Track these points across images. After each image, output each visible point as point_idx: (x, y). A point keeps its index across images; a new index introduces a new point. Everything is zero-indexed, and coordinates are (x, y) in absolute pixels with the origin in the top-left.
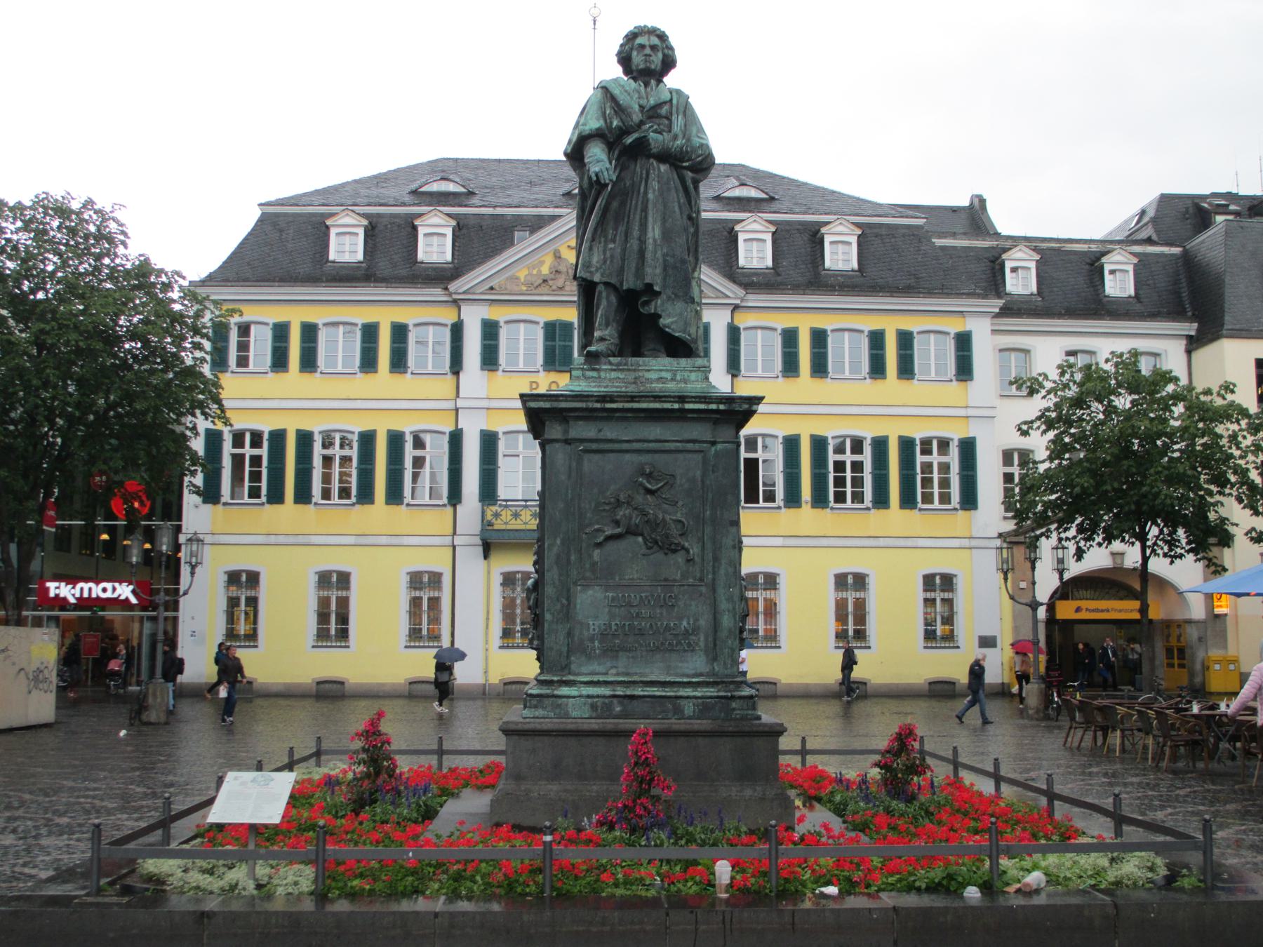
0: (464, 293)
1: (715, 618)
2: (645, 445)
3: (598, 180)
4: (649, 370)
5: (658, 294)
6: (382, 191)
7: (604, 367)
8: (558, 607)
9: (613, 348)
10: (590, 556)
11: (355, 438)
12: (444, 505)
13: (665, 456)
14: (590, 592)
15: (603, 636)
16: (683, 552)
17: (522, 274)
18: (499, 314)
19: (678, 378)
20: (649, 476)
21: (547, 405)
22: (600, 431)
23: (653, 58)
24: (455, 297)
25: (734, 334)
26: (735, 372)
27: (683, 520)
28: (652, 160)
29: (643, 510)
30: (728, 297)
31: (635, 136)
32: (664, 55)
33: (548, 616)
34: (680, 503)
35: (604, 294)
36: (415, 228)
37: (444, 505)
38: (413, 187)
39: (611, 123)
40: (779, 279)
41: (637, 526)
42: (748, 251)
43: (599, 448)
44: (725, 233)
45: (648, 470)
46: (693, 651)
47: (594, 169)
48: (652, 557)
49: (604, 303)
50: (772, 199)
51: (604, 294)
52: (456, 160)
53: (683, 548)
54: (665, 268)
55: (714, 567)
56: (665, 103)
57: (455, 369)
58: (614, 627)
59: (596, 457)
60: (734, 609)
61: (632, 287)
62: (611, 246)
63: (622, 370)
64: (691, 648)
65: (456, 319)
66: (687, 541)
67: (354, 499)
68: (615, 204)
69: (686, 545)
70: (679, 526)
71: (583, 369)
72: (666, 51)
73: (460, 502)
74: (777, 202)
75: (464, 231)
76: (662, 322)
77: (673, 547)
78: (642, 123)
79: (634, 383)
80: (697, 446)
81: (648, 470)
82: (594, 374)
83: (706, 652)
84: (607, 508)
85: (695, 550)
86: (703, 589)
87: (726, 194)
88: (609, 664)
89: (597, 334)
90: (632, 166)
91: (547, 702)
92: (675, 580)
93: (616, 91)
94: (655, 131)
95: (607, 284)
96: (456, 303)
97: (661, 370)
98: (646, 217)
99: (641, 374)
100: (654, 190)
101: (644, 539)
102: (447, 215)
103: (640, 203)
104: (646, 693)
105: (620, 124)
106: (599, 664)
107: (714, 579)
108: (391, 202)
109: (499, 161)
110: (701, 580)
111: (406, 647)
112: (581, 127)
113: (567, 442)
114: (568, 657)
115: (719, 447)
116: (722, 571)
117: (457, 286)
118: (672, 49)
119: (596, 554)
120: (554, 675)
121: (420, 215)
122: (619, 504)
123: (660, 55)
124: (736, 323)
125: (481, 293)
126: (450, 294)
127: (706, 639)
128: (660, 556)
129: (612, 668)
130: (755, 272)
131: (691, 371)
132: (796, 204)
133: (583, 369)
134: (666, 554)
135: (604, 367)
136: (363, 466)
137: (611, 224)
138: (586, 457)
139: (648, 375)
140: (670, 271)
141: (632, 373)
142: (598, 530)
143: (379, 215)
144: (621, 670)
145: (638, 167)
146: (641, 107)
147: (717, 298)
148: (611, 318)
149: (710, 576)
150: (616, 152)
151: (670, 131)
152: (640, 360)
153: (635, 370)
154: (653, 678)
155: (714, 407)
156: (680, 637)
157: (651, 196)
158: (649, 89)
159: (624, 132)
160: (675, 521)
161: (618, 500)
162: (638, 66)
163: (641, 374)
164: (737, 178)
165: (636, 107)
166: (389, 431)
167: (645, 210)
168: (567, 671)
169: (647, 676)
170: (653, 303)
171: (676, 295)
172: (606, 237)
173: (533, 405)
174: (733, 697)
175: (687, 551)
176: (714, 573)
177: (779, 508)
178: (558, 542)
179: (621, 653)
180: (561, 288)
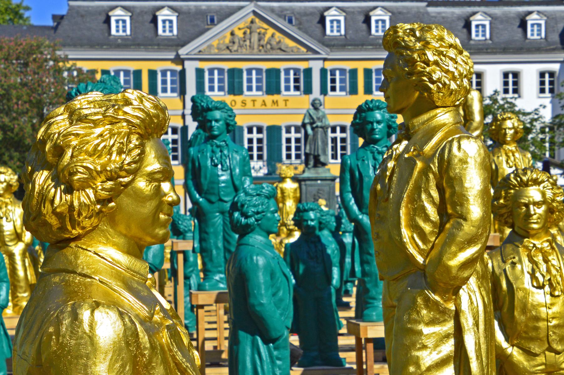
0: (187, 54)
12: (179, 164)
17: (215, 43)
18: (205, 66)
25: (323, 72)
43: (311, 185)
117: (183, 52)
125: (195, 54)
130: (334, 38)
145: (316, 129)
180: (237, 51)
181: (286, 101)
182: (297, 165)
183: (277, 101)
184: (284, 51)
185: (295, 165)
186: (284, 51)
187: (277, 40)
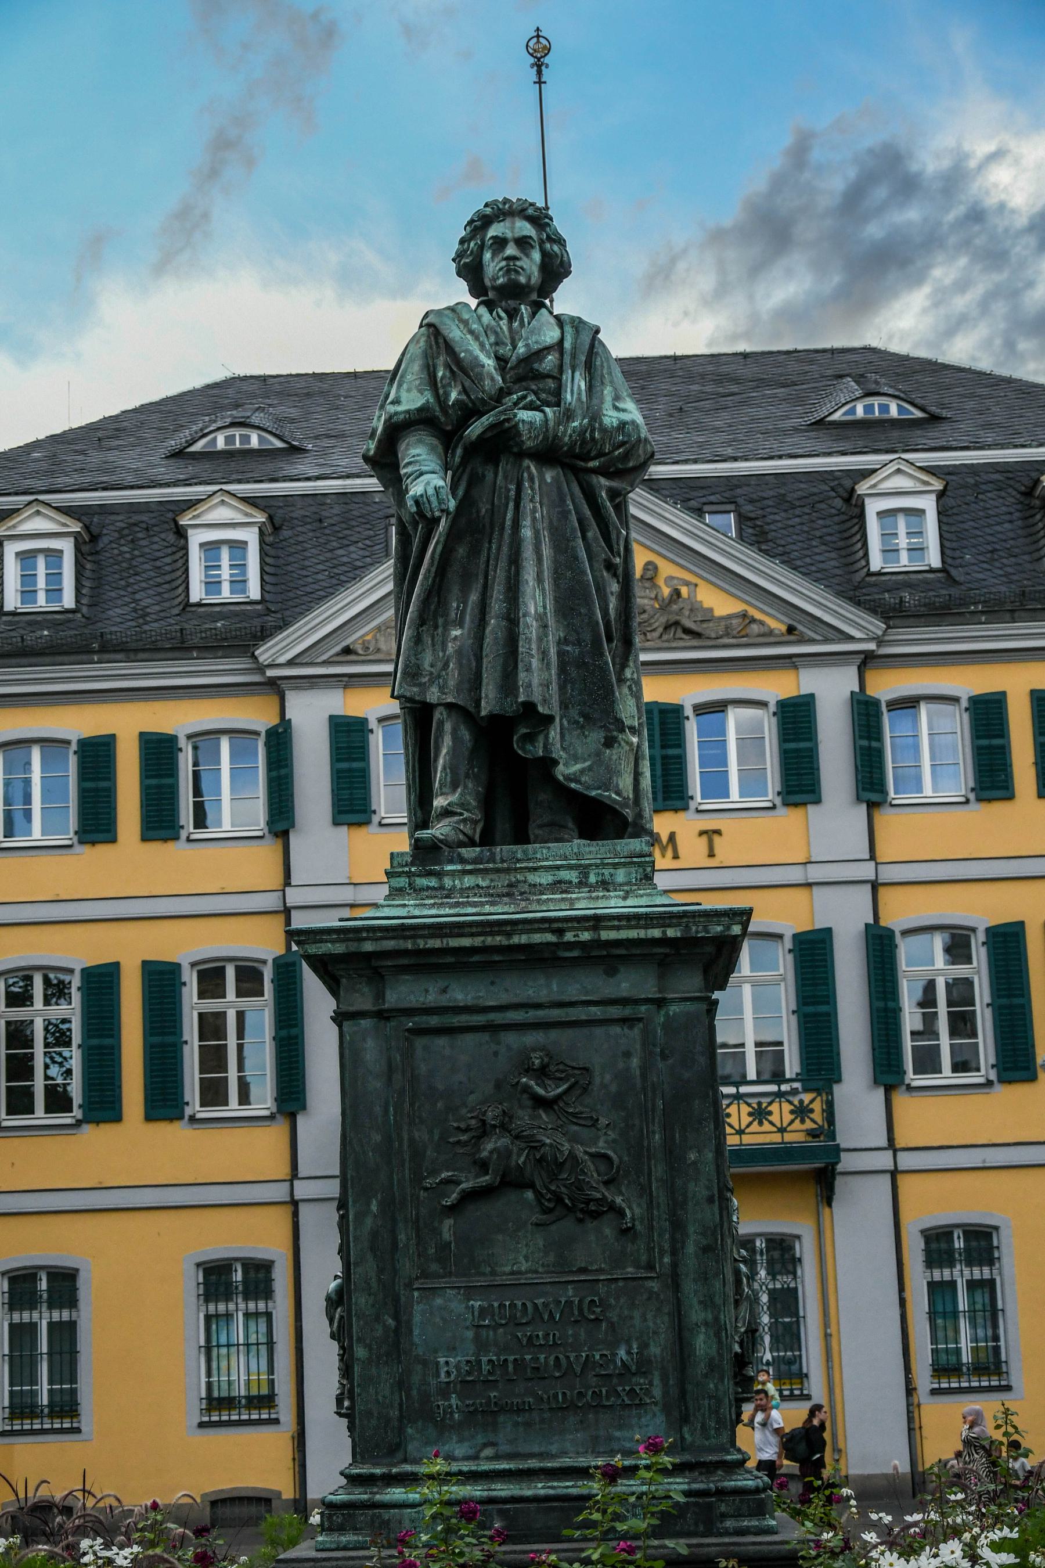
0: (291, 663)
1: (681, 1338)
2: (532, 1015)
3: (420, 513)
4: (535, 869)
5: (549, 719)
6: (111, 456)
7: (449, 868)
8: (379, 1332)
9: (467, 829)
10: (437, 1232)
11: (76, 981)
13: (570, 1033)
14: (439, 1301)
15: (465, 1386)
16: (611, 1216)
19: (592, 879)
20: (542, 1073)
21: (339, 948)
22: (444, 991)
23: (524, 263)
24: (270, 673)
26: (874, 797)
27: (610, 1153)
28: (527, 462)
29: (530, 1139)
30: (851, 638)
31: (486, 420)
32: (544, 254)
33: (360, 1352)
34: (603, 1121)
35: (448, 727)
36: (181, 533)
37: (272, 1117)
38: (174, 443)
39: (447, 395)
40: (955, 592)
41: (520, 1169)
42: (888, 536)
44: (838, 503)
45: (537, 1062)
46: (639, 1406)
47: (416, 489)
48: (553, 1228)
49: (447, 742)
50: (934, 419)
51: (448, 727)
52: (264, 379)
53: (613, 1208)
54: (562, 669)
55: (673, 1240)
56: (548, 349)
57: (280, 827)
58: (485, 1368)
59: (441, 1041)
60: (716, 1319)
61: (497, 710)
62: (456, 632)
63: (485, 871)
64: (637, 1403)
65: (274, 720)
66: (621, 1193)
67: (77, 1113)
68: (461, 551)
69: (619, 1200)
70: (603, 1168)
71: (409, 875)
72: (548, 246)
73: (304, 1107)
74: (945, 426)
75: (286, 533)
76: (562, 771)
77: (592, 1207)
78: (502, 393)
79: (508, 895)
80: (627, 1011)
81: (537, 1062)
82: (433, 882)
83: (667, 1409)
84: (464, 1138)
85: (633, 1211)
86: (655, 1286)
87: (836, 416)
88: (480, 1439)
89: (439, 802)
90: (490, 476)
91: (362, 1517)
92: (600, 1271)
93: (455, 333)
94: (530, 407)
95: (450, 706)
96: (276, 688)
97: (558, 868)
98: (518, 573)
99: (520, 877)
100: (534, 519)
101: (538, 1195)
102: (245, 500)
103: (505, 549)
104: (551, 1492)
105: (464, 397)
106: (461, 1441)
107: (674, 1265)
108: (130, 479)
109: (355, 375)
110: (650, 1267)
111: (202, 1425)
112: (391, 409)
113: (382, 1015)
114: (401, 1430)
115: (674, 1009)
116: (691, 1248)
118: (561, 242)
119: (447, 1227)
120: (375, 1465)
121: (191, 504)
122: (484, 1131)
123: (536, 256)
124: (870, 692)
125: (326, 663)
126: (261, 669)
127: (664, 1379)
128: (568, 1225)
129: (485, 1445)
130: (906, 581)
131: (615, 866)
132: (987, 426)
133: (409, 875)
134: (581, 1221)
135: (449, 868)
136: (95, 1042)
137: (456, 590)
138: (420, 1042)
139: (533, 878)
140: (574, 673)
141: (502, 875)
142: (448, 1181)
143: (104, 509)
144: (505, 1448)
145: (499, 476)
146: (501, 361)
147: (826, 641)
148: (462, 770)
149: (667, 1260)
150: (459, 451)
151: (558, 405)
152: (519, 850)
153: (507, 871)
154: (566, 1461)
155: (656, 933)
156: (615, 1381)
157: (527, 533)
158: (516, 324)
159: (470, 411)
160: (591, 1155)
161: (484, 1122)
162: (495, 279)
163: (520, 877)
164: (859, 379)
165: (489, 363)
166: (145, 963)
167: (515, 561)
168: (400, 1455)
169: (552, 1457)
170: (541, 738)
171: (587, 717)
172: (446, 615)
173: (313, 949)
174: (721, 1493)
175: (621, 1213)
176: (674, 1253)
177: (989, 1083)
178: (374, 1207)
179: (501, 1419)
181: (710, 835)
182: (765, 1101)
183: (672, 837)
184: (697, 635)
185: (754, 1101)
186: (697, 635)
187: (666, 591)
